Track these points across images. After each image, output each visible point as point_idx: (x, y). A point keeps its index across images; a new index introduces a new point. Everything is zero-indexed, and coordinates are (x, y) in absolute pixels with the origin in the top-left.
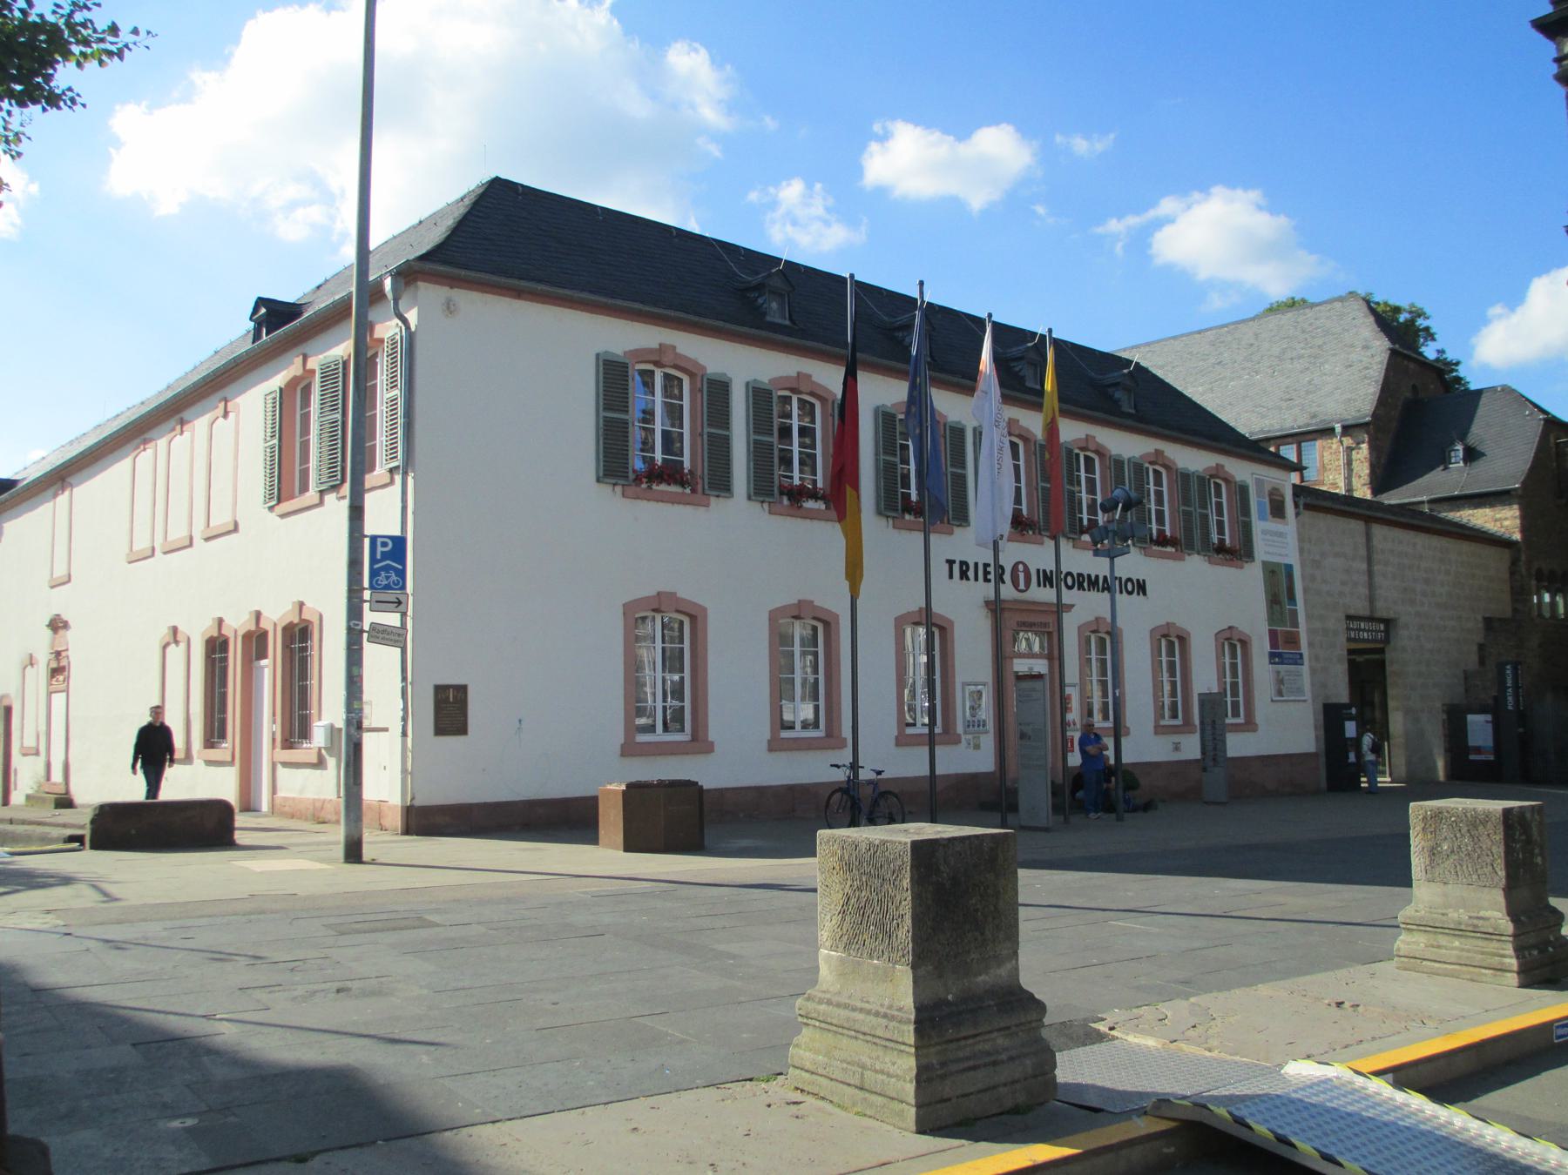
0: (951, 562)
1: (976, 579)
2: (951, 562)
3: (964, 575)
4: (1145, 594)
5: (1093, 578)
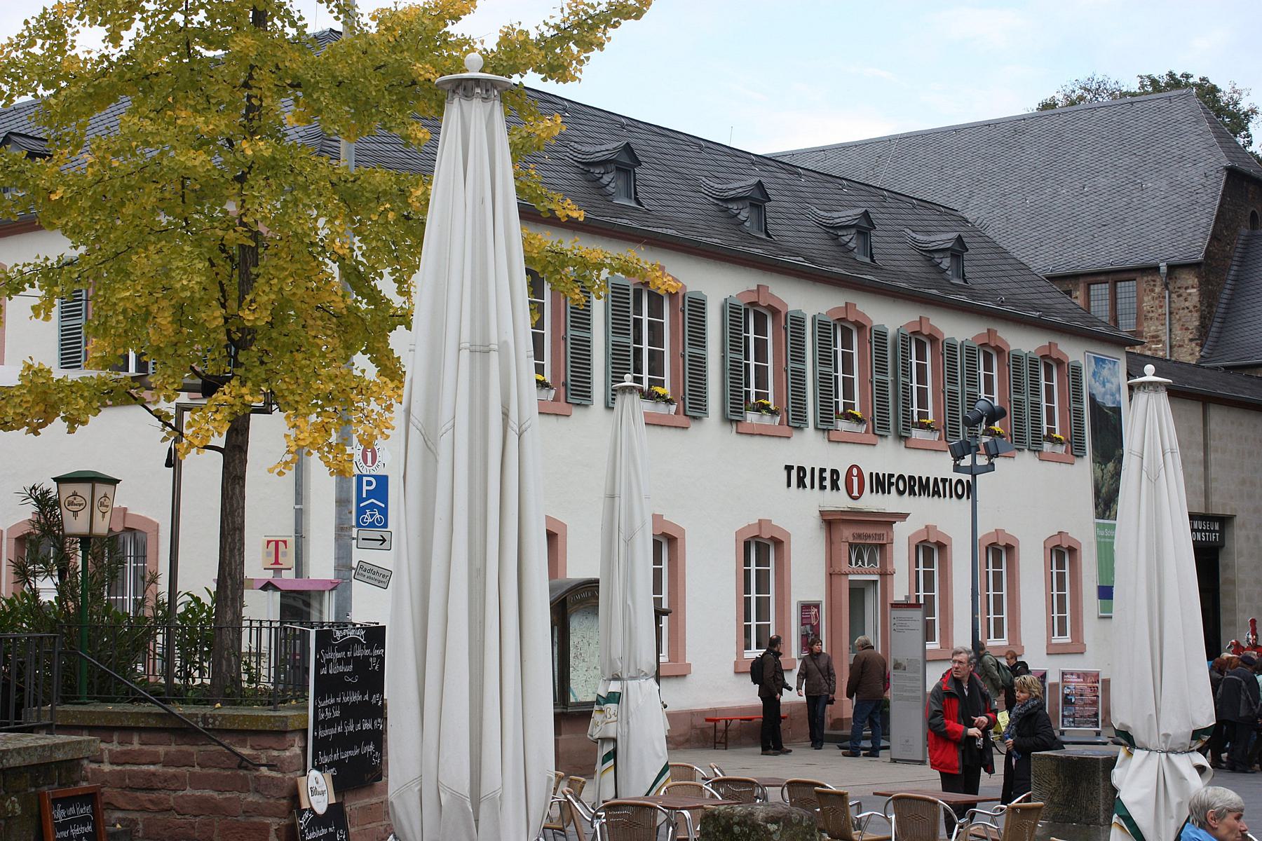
1: (812, 487)
2: (789, 468)
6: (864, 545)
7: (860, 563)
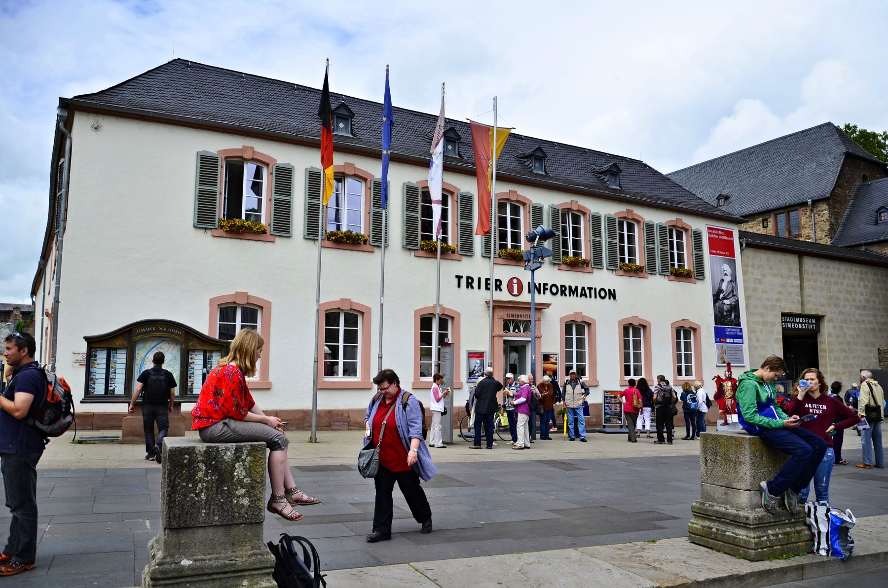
0: (459, 278)
1: (479, 287)
2: (459, 278)
3: (469, 284)
4: (614, 298)
5: (573, 289)
6: (520, 321)
7: (517, 331)
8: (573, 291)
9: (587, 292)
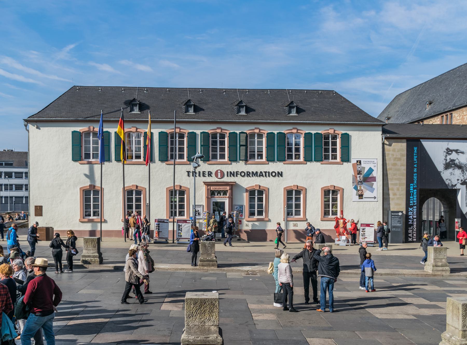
0: (188, 172)
2: (188, 172)
4: (281, 176)
5: (255, 173)
6: (221, 191)
8: (255, 174)
9: (264, 174)
